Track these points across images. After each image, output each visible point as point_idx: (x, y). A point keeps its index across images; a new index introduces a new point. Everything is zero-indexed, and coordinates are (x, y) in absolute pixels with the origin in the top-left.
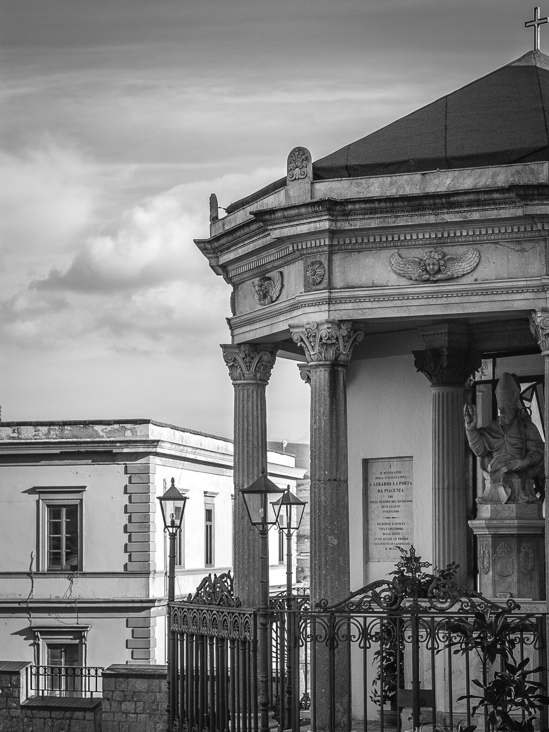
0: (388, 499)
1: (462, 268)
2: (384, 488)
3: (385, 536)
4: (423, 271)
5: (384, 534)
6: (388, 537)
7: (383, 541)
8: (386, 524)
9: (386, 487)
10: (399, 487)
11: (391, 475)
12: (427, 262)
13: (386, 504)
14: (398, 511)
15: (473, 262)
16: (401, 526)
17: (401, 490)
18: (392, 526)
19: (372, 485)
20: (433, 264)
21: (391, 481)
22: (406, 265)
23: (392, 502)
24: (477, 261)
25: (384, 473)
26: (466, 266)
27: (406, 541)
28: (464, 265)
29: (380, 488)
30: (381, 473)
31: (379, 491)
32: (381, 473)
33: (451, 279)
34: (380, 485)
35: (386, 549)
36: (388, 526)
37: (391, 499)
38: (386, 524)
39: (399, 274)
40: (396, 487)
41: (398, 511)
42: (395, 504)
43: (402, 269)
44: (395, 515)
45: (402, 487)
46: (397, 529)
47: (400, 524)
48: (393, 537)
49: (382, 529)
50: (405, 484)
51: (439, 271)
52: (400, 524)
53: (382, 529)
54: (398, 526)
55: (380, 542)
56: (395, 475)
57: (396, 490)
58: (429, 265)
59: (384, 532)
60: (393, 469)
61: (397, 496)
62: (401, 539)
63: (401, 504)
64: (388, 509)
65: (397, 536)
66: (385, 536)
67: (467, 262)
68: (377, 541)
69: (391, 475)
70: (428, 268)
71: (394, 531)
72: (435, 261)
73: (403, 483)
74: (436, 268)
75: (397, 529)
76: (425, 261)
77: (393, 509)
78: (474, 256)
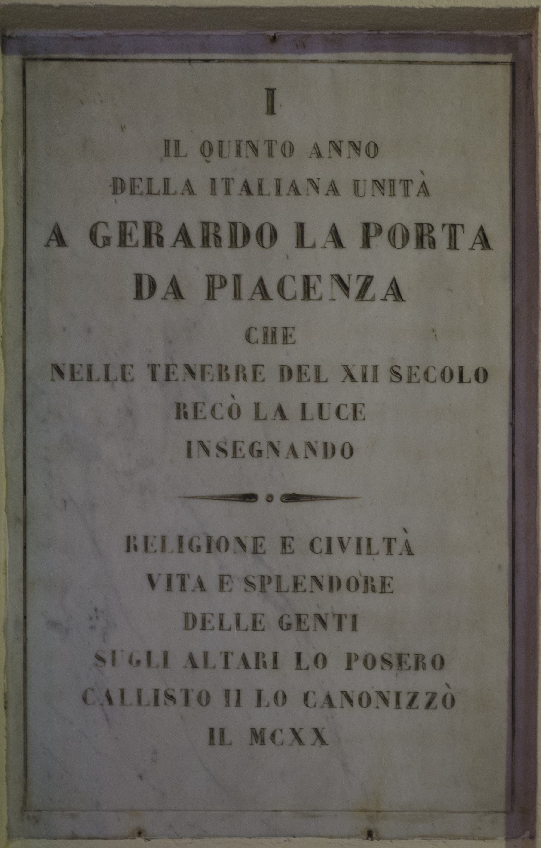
0: (247, 356)
2: (195, 265)
3: (214, 642)
5: (190, 621)
6: (243, 643)
7: (178, 678)
8: (212, 545)
9: (226, 260)
10: (353, 261)
11: (282, 168)
13: (216, 392)
14: (348, 451)
16: (376, 566)
17: (380, 287)
18: (274, 563)
19: (76, 237)
21: (282, 213)
23: (285, 373)
25: (207, 150)
27: (426, 681)
29: (159, 263)
30: (172, 148)
31: (144, 287)
32: (172, 148)
34: (152, 236)
35: (216, 736)
36: (238, 564)
37: (275, 355)
38: (212, 545)
40: (322, 261)
41: (348, 451)
42: (311, 393)
44: (308, 475)
45: (386, 262)
46: (334, 584)
47: (364, 546)
48: (288, 643)
49: (177, 582)
50: (424, 237)
52: (364, 546)
53: (177, 582)
54: (347, 565)
55: (151, 680)
56: (313, 168)
57: (324, 287)
59: (196, 604)
60: (294, 123)
61: (329, 332)
62: (370, 662)
63: (370, 394)
64: (246, 430)
65: (334, 643)
66: (214, 642)
68: (115, 678)
69: (282, 168)
71: (308, 603)
73: (398, 237)
75: (334, 584)
77: (284, 433)
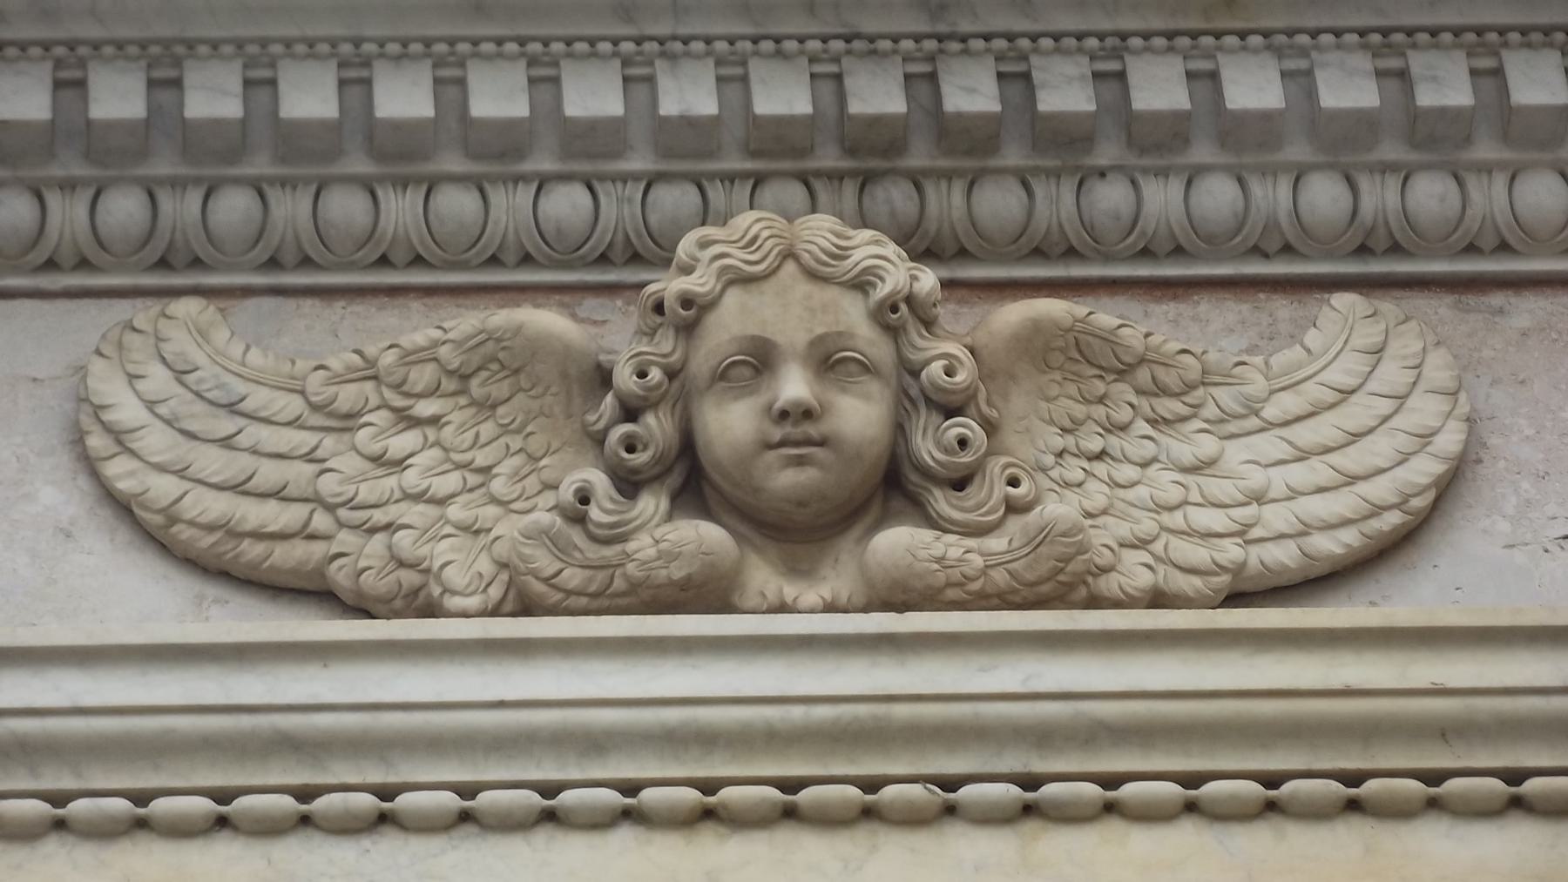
1: (1218, 488)
4: (629, 484)
12: (734, 320)
15: (1379, 449)
20: (829, 361)
22: (348, 421)
24: (1450, 440)
26: (1300, 474)
28: (1247, 460)
33: (1063, 581)
39: (219, 568)
43: (269, 474)
51: (894, 486)
58: (760, 359)
67: (1305, 434)
70: (730, 423)
72: (853, 315)
74: (859, 415)
76: (696, 309)
78: (1392, 374)
